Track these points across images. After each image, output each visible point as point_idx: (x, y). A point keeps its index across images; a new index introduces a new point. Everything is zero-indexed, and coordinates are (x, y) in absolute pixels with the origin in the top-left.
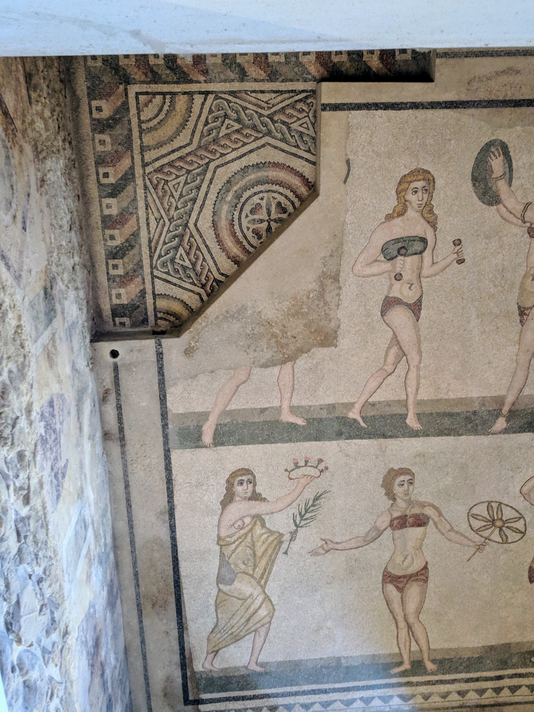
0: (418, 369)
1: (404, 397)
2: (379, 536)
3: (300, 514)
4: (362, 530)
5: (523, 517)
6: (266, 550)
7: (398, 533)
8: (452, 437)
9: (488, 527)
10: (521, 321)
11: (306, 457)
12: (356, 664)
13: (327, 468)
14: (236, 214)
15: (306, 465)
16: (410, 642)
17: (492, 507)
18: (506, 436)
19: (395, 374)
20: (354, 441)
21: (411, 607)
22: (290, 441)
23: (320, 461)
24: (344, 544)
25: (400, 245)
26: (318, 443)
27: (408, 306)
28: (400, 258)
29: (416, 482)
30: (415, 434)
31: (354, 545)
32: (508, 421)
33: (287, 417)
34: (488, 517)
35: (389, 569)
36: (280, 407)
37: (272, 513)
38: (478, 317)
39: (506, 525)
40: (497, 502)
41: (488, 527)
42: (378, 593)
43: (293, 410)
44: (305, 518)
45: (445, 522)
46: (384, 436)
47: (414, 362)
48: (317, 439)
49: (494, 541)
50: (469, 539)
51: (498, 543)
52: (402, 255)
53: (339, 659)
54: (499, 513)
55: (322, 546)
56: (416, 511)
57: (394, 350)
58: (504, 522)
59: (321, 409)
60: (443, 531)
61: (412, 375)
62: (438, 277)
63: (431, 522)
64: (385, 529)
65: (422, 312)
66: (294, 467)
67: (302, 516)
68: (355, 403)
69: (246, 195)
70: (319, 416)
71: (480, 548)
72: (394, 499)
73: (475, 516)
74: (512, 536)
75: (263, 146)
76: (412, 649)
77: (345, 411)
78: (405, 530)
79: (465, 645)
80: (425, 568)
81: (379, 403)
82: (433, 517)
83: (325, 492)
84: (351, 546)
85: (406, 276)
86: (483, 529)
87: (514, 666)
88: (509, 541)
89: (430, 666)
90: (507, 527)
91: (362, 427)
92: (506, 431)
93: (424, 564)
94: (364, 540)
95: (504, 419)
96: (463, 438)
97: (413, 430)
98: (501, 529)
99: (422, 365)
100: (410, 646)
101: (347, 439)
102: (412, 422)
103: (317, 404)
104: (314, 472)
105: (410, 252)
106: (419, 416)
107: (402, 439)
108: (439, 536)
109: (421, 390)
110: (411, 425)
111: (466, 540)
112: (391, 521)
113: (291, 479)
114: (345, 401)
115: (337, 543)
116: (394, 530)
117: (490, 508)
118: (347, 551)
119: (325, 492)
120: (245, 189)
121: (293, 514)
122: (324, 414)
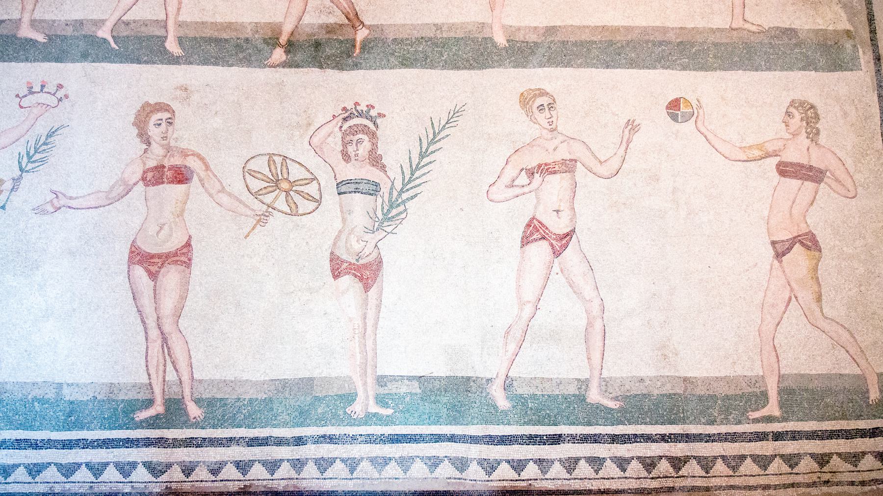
1: (162, 17)
2: (127, 193)
3: (28, 154)
4: (104, 184)
5: (315, 179)
7: (152, 190)
9: (271, 189)
11: (43, 81)
12: (85, 398)
13: (66, 96)
15: (42, 90)
16: (165, 365)
17: (274, 161)
18: (287, 70)
20: (103, 64)
22: (27, 60)
23: (60, 86)
24: (80, 199)
26: (59, 64)
29: (177, 121)
30: (174, 60)
31: (93, 204)
32: (287, 52)
33: (26, 32)
34: (273, 178)
36: (20, 20)
39: (294, 189)
41: (271, 189)
42: (122, 279)
43: (34, 23)
44: (33, 159)
45: (214, 178)
46: (139, 62)
48: (58, 60)
49: (279, 211)
50: (246, 206)
53: (60, 386)
54: (285, 170)
55: (51, 201)
56: (177, 161)
59: (67, 25)
60: (213, 192)
63: (195, 179)
67: (29, 157)
70: (63, 33)
71: (262, 219)
72: (149, 144)
73: (253, 173)
76: (167, 379)
77: (94, 29)
78: (161, 186)
80: (188, 245)
81: (134, 21)
82: (198, 171)
84: (89, 204)
86: (264, 191)
87: (321, 421)
88: (300, 212)
89: (194, 411)
90: (296, 191)
91: (113, 49)
93: (186, 239)
94: (107, 198)
95: (283, 50)
96: (234, 69)
97: (173, 55)
100: (165, 371)
101: (94, 61)
103: (62, 19)
108: (205, 197)
109: (183, 11)
110: (171, 50)
111: (241, 206)
112: (144, 172)
113: (21, 107)
114: (95, 17)
115: (71, 198)
116: (147, 185)
117: (272, 162)
118: (83, 211)
121: (19, 154)
122: (69, 31)
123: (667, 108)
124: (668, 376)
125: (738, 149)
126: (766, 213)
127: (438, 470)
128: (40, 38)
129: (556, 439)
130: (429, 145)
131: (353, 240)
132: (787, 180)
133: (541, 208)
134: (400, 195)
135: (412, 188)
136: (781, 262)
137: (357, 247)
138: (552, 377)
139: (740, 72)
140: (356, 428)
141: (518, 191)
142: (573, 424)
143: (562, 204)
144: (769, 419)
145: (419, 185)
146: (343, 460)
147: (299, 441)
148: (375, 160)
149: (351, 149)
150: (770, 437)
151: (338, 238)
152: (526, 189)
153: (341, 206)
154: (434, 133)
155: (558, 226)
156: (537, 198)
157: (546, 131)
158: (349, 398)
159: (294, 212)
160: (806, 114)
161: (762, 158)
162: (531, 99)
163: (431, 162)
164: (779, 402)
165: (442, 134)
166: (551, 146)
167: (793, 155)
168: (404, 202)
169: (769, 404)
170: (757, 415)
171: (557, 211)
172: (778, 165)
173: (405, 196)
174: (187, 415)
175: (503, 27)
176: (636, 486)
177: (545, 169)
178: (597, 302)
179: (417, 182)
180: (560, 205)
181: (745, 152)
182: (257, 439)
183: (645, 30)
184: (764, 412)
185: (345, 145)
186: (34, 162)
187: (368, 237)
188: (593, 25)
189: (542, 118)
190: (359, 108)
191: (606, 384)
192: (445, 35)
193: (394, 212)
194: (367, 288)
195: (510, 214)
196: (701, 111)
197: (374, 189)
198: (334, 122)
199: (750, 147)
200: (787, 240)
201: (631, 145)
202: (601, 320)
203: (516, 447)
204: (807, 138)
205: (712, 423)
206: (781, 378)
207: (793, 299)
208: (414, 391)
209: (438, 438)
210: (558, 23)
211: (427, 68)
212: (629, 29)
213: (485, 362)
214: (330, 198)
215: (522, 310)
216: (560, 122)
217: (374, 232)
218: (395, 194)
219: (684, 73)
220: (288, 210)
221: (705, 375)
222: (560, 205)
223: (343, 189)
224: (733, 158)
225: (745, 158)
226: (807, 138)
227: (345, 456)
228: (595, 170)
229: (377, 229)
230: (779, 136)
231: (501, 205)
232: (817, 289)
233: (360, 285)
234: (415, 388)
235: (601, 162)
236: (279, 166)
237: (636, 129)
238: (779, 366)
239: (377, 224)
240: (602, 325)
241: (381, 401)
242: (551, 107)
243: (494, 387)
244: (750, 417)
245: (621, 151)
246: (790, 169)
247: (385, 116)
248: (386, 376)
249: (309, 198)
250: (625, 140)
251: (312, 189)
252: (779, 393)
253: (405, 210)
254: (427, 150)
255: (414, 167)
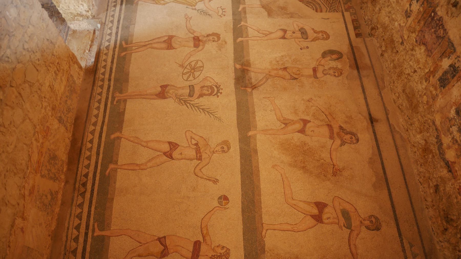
0: (260, 40)
1: (250, 36)
3: (203, 11)
5: (195, 79)
6: (189, 2)
8: (233, 52)
10: (281, 68)
13: (221, 17)
14: (306, 2)
16: (137, 46)
18: (233, 69)
19: (259, 34)
21: (155, 45)
25: (305, 32)
27: (284, 35)
28: (300, 33)
30: (235, 40)
35: (175, 37)
37: (204, 4)
38: (282, 55)
40: (203, 69)
42: (164, 34)
47: (263, 39)
48: (233, 14)
49: (184, 70)
51: (183, 72)
52: (301, 33)
53: (134, 24)
54: (198, 71)
55: (188, 17)
56: (201, 43)
57: (267, 33)
58: (193, 73)
61: (258, 38)
62: (295, 43)
63: (195, 49)
64: (194, 35)
65: (282, 40)
66: (222, 8)
67: (202, 11)
68: (247, 23)
69: (311, 4)
71: (182, 66)
74: (185, 77)
75: (326, 8)
78: (193, 41)
79: (131, 65)
80: (174, 48)
81: (247, 30)
82: (198, 49)
83: (212, 17)
85: (294, 35)
88: (183, 75)
89: (123, 54)
90: (190, 74)
92: (235, 69)
93: (176, 48)
98: (189, 72)
99: (262, 41)
101: (233, 22)
102: (240, 39)
104: (220, 14)
105: (303, 35)
106: (242, 41)
107: (233, 37)
110: (239, 38)
113: (218, 8)
115: (189, 21)
119: (212, 17)
120: (314, 4)
123: (224, 195)
124: (115, 192)
125: (206, 224)
126: (178, 235)
127: (94, 118)
128: (240, 9)
129: (98, 154)
130: (207, 112)
131: (173, 91)
132: (193, 245)
133: (183, 148)
134: (188, 103)
135: (191, 107)
136: (157, 240)
137: (171, 91)
138: (120, 152)
139: (242, 227)
140: (111, 94)
141: (189, 140)
142: (102, 159)
143: (184, 155)
144: (93, 231)
145: (192, 109)
146: (102, 91)
147: (110, 80)
148: (201, 96)
149: (205, 88)
150: (86, 231)
151: (174, 86)
152: (190, 143)
153: (185, 86)
154: (212, 113)
155: (175, 154)
156: (186, 147)
157: (213, 149)
158: (121, 92)
159: (183, 74)
160: (223, 256)
161: (202, 234)
162: (226, 144)
163: (200, 112)
164: (100, 235)
165: (211, 115)
166: (207, 151)
167: (204, 248)
168: (186, 104)
169: (99, 231)
170: (96, 226)
171: (181, 154)
172: (199, 241)
173: (188, 105)
174: (122, 53)
175: (255, 135)
176: (77, 180)
177: (198, 151)
178: (145, 167)
179: (193, 108)
180: (183, 154)
181: (205, 227)
182: (112, 70)
183: (258, 187)
184: (97, 229)
185: (207, 86)
186: (201, 12)
187: (174, 95)
188: (259, 166)
189: (219, 148)
190: (220, 90)
191: (115, 170)
192: (250, 115)
193: (182, 102)
194: (156, 95)
195: (180, 138)
196: (223, 209)
197: (191, 95)
198: (215, 83)
199: (207, 230)
200: (166, 243)
201: (208, 181)
202: (138, 169)
203: (97, 140)
204: (212, 256)
205: (95, 208)
206: (109, 237)
207: (141, 244)
208: (121, 110)
209: (104, 117)
210: (259, 154)
211: (237, 110)
212: (259, 180)
213: (128, 131)
214: (188, 83)
215: (145, 142)
216: (217, 154)
217: (175, 96)
218: (189, 102)
219: (240, 203)
220: (185, 72)
221: (114, 206)
222: (183, 154)
223: (191, 87)
224: (203, 222)
225: (202, 227)
226: (212, 256)
227: (103, 92)
228: (198, 167)
229: (176, 97)
230: (213, 242)
231: (184, 135)
232: (144, 255)
233: (158, 93)
234: (121, 110)
235: (200, 169)
236: (200, 69)
237: (215, 183)
238: (114, 236)
239: (178, 97)
240: (137, 169)
241: (118, 101)
242: (224, 151)
243: (119, 134)
244: (95, 224)
245: (205, 177)
246: (197, 247)
247: (218, 97)
248: (126, 102)
249: (189, 77)
250: (210, 178)
251: (191, 78)
252: (103, 236)
253: (183, 105)
254: (205, 111)
255: (199, 107)
